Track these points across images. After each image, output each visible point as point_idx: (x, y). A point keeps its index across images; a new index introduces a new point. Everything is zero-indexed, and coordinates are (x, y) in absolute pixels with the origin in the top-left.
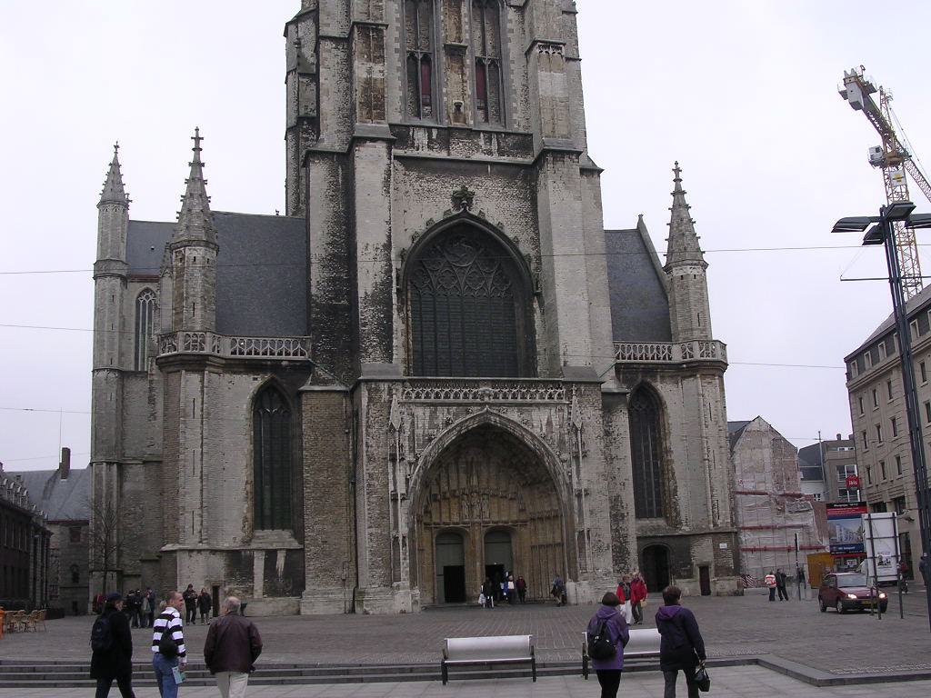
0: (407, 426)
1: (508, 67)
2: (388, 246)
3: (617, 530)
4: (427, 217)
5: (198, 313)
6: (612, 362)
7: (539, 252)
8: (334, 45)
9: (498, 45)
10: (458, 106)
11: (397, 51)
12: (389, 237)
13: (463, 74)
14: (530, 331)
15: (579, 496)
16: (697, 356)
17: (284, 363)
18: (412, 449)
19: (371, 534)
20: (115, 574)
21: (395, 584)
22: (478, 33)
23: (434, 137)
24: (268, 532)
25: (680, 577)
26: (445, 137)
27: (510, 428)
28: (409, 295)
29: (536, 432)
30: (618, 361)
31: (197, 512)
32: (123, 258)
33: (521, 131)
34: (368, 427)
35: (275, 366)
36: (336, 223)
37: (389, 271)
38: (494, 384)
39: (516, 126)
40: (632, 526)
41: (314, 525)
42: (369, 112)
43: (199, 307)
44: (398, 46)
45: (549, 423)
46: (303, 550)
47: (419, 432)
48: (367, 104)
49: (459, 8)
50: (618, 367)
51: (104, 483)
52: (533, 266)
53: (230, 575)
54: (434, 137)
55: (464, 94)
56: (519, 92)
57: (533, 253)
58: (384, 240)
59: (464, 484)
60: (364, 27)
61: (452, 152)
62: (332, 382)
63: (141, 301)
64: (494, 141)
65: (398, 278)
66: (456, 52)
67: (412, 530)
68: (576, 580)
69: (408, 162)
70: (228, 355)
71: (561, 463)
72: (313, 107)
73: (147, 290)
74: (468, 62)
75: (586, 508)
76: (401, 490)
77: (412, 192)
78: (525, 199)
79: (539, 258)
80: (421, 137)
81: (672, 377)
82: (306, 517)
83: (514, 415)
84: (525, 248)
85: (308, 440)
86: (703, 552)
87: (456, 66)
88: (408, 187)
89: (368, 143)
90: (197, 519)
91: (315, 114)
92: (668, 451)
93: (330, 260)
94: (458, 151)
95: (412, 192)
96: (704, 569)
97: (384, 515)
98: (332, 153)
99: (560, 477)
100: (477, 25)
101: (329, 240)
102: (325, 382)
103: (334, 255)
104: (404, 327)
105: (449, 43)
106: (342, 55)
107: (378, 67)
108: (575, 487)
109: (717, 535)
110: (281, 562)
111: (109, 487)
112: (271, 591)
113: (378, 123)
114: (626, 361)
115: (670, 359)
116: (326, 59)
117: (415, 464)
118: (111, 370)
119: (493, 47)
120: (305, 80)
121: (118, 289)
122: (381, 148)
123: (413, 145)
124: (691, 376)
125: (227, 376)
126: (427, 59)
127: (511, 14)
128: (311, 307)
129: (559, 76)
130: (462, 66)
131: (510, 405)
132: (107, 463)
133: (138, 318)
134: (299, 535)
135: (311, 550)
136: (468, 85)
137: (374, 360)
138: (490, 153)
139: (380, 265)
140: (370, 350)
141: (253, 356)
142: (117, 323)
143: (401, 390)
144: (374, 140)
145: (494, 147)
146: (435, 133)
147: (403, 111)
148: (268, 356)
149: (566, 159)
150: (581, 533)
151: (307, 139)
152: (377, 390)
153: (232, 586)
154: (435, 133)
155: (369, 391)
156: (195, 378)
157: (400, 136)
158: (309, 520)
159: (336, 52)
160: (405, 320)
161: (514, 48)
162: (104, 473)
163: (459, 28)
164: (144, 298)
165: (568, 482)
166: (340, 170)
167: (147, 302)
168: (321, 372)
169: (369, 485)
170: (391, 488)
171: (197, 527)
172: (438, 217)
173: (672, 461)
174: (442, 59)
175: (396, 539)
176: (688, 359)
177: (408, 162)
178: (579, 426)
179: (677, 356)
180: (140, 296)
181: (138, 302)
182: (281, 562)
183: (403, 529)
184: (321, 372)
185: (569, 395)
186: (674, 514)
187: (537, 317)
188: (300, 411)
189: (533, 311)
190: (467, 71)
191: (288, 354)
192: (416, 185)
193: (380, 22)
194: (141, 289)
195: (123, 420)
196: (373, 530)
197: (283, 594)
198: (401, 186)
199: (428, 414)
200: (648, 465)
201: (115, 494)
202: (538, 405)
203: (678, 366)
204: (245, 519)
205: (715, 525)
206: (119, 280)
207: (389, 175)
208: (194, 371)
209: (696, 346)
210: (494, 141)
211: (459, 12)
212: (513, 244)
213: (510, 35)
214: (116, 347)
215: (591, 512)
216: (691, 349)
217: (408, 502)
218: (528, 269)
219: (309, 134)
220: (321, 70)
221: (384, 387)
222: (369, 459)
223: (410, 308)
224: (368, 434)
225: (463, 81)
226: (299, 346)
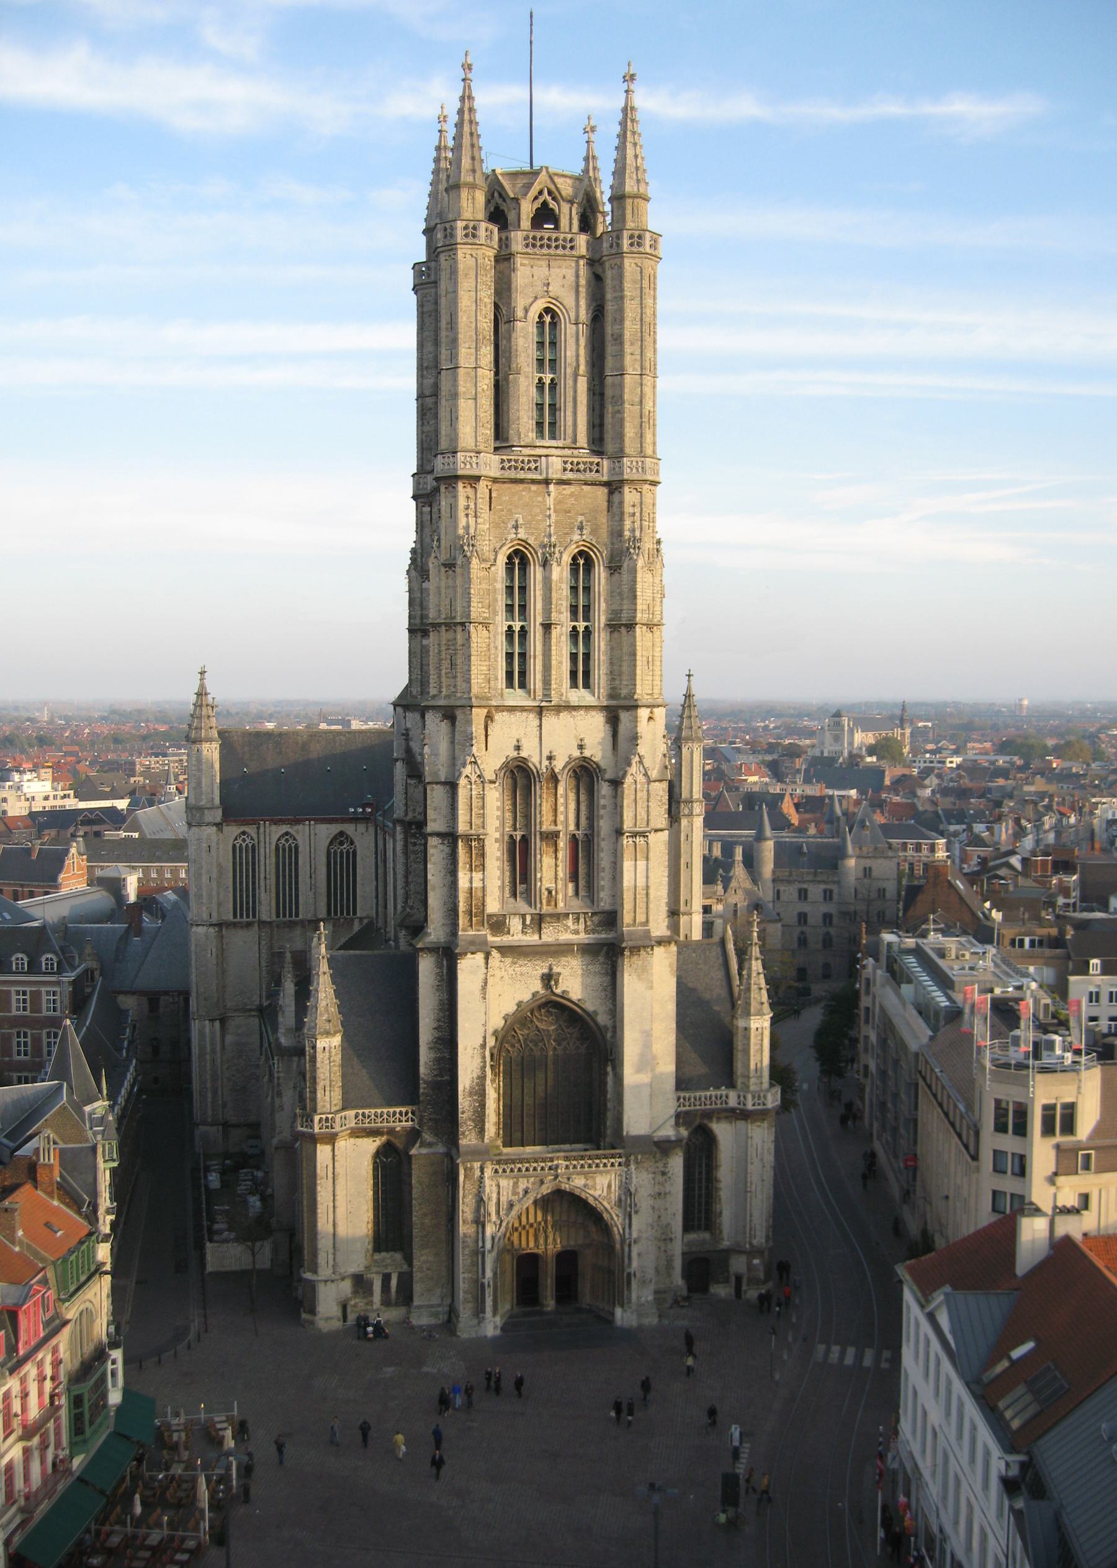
0: (494, 1196)
1: (598, 845)
2: (483, 1046)
3: (665, 1251)
4: (519, 998)
5: (327, 1093)
6: (672, 1112)
7: (615, 1022)
8: (440, 841)
9: (591, 818)
10: (550, 892)
11: (497, 840)
12: (485, 1038)
13: (556, 858)
14: (603, 1091)
15: (630, 1245)
16: (750, 1107)
17: (398, 1129)
18: (498, 1212)
19: (464, 1278)
20: (220, 1127)
21: (481, 1315)
22: (572, 806)
23: (528, 922)
24: (384, 1254)
25: (718, 1282)
26: (539, 921)
27: (577, 1192)
28: (501, 1068)
29: (597, 1194)
30: (679, 1109)
31: (331, 1251)
32: (217, 801)
33: (607, 907)
34: (464, 1197)
35: (391, 1131)
36: (440, 1010)
37: (484, 1067)
38: (566, 1159)
39: (602, 904)
40: (677, 1249)
41: (423, 1258)
42: (471, 920)
43: (328, 1089)
44: (497, 835)
45: (609, 1186)
46: (411, 1273)
47: (503, 1199)
48: (470, 913)
49: (556, 788)
50: (678, 1116)
51: (208, 1039)
52: (609, 1035)
53: (355, 1292)
54: (528, 922)
55: (556, 878)
56: (607, 870)
57: (609, 1024)
58: (481, 1041)
59: (539, 1219)
60: (468, 839)
61: (542, 936)
62: (436, 1144)
63: (238, 845)
64: (582, 920)
65: (492, 1055)
66: (551, 837)
67: (495, 1274)
68: (622, 1306)
69: (506, 950)
70: (353, 1125)
71: (615, 1218)
72: (420, 810)
73: (244, 833)
74: (561, 844)
75: (634, 1254)
76: (488, 1245)
77: (506, 977)
78: (607, 974)
79: (614, 1027)
80: (515, 924)
81: (727, 1117)
82: (414, 1251)
83: (578, 1182)
84: (603, 1019)
85: (415, 1193)
86: (738, 1264)
87: (552, 850)
88: (503, 973)
89: (469, 955)
90: (331, 1257)
91: (420, 818)
92: (718, 1181)
93: (436, 1043)
94: (551, 934)
95: (506, 977)
96: (739, 1279)
97: (474, 1264)
98: (438, 948)
99: (615, 1229)
100: (572, 796)
101: (435, 1025)
102: (430, 1145)
103: (439, 1038)
104: (495, 1095)
105: (544, 828)
106: (447, 850)
107: (477, 876)
108: (627, 1236)
109: (753, 1252)
110: (394, 1282)
111: (213, 1044)
112: (386, 1302)
113: (479, 931)
114: (687, 1108)
115: (726, 1103)
116: (433, 855)
117: (500, 1225)
118: (211, 925)
119: (587, 818)
120: (412, 782)
121: (214, 838)
122: (480, 957)
123: (508, 933)
124: (742, 1119)
125: (352, 1140)
126: (525, 840)
127: (605, 789)
128: (419, 1084)
129: (641, 864)
130: (556, 851)
131: (578, 1174)
132: (210, 1020)
133: (234, 863)
134: (409, 1259)
135: (417, 1276)
136: (560, 869)
137: (470, 1140)
138: (577, 932)
139: (478, 1061)
140: (467, 1133)
141: (373, 1125)
142: (214, 876)
143: (490, 1167)
144: (473, 953)
145: (582, 926)
146: (528, 918)
147: (503, 902)
148: (385, 1124)
149: (642, 952)
150: (629, 1274)
151: (415, 844)
152: (472, 1168)
153: (357, 1300)
154: (528, 919)
155: (465, 1170)
156: (328, 1148)
157: (498, 925)
158: (416, 1252)
159: (441, 847)
160: (498, 1090)
161: (604, 826)
162: (207, 1030)
163: (555, 810)
164: (240, 841)
165: (621, 1231)
166: (445, 962)
167: (244, 845)
168: (427, 1137)
169: (463, 1242)
170: (480, 1244)
171: (331, 1262)
172: (526, 997)
173: (720, 1189)
174: (537, 843)
175: (483, 1285)
176: (741, 1106)
177: (504, 950)
178: (633, 1190)
179: (733, 1102)
180: (236, 839)
181: (234, 846)
182: (394, 1282)
183: (489, 1274)
184: (427, 1137)
185: (627, 1164)
186: (718, 1232)
187: (610, 1079)
188: (410, 1168)
189: (606, 1074)
190: (560, 855)
191: (400, 1121)
192: (511, 971)
193: (481, 831)
194: (236, 834)
195: (224, 971)
196: (466, 1275)
197: (397, 1304)
198: (498, 974)
199: (511, 1184)
200: (700, 1188)
201: (218, 1048)
202: (601, 1173)
203: (733, 1110)
204: (368, 1250)
205: (751, 1244)
206: (214, 828)
207: (486, 983)
208: (326, 1143)
209: (749, 1097)
210: (582, 920)
211: (556, 794)
212: (592, 1016)
213: (602, 812)
214: (215, 900)
215: (639, 1255)
216: (745, 1097)
217: (494, 1253)
218: (604, 1038)
219: (417, 838)
220: (429, 866)
221: (477, 1165)
222: (464, 1222)
223: (501, 1079)
224: (463, 1203)
225: (556, 865)
226: (410, 1114)
